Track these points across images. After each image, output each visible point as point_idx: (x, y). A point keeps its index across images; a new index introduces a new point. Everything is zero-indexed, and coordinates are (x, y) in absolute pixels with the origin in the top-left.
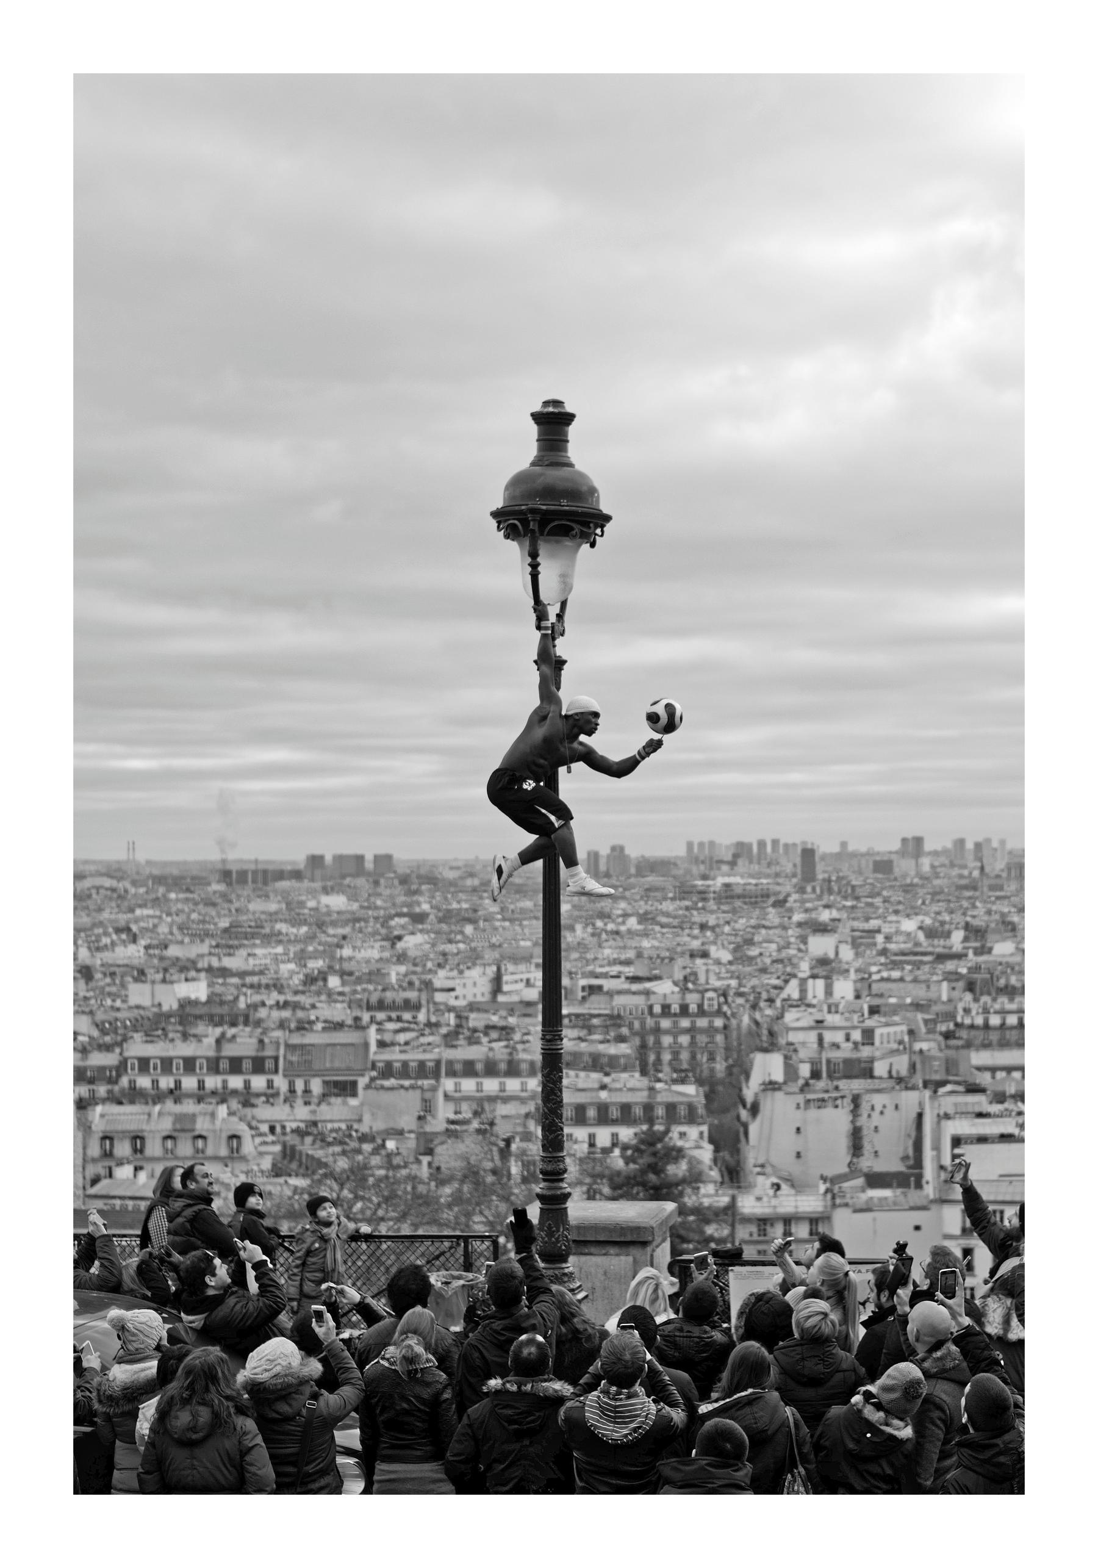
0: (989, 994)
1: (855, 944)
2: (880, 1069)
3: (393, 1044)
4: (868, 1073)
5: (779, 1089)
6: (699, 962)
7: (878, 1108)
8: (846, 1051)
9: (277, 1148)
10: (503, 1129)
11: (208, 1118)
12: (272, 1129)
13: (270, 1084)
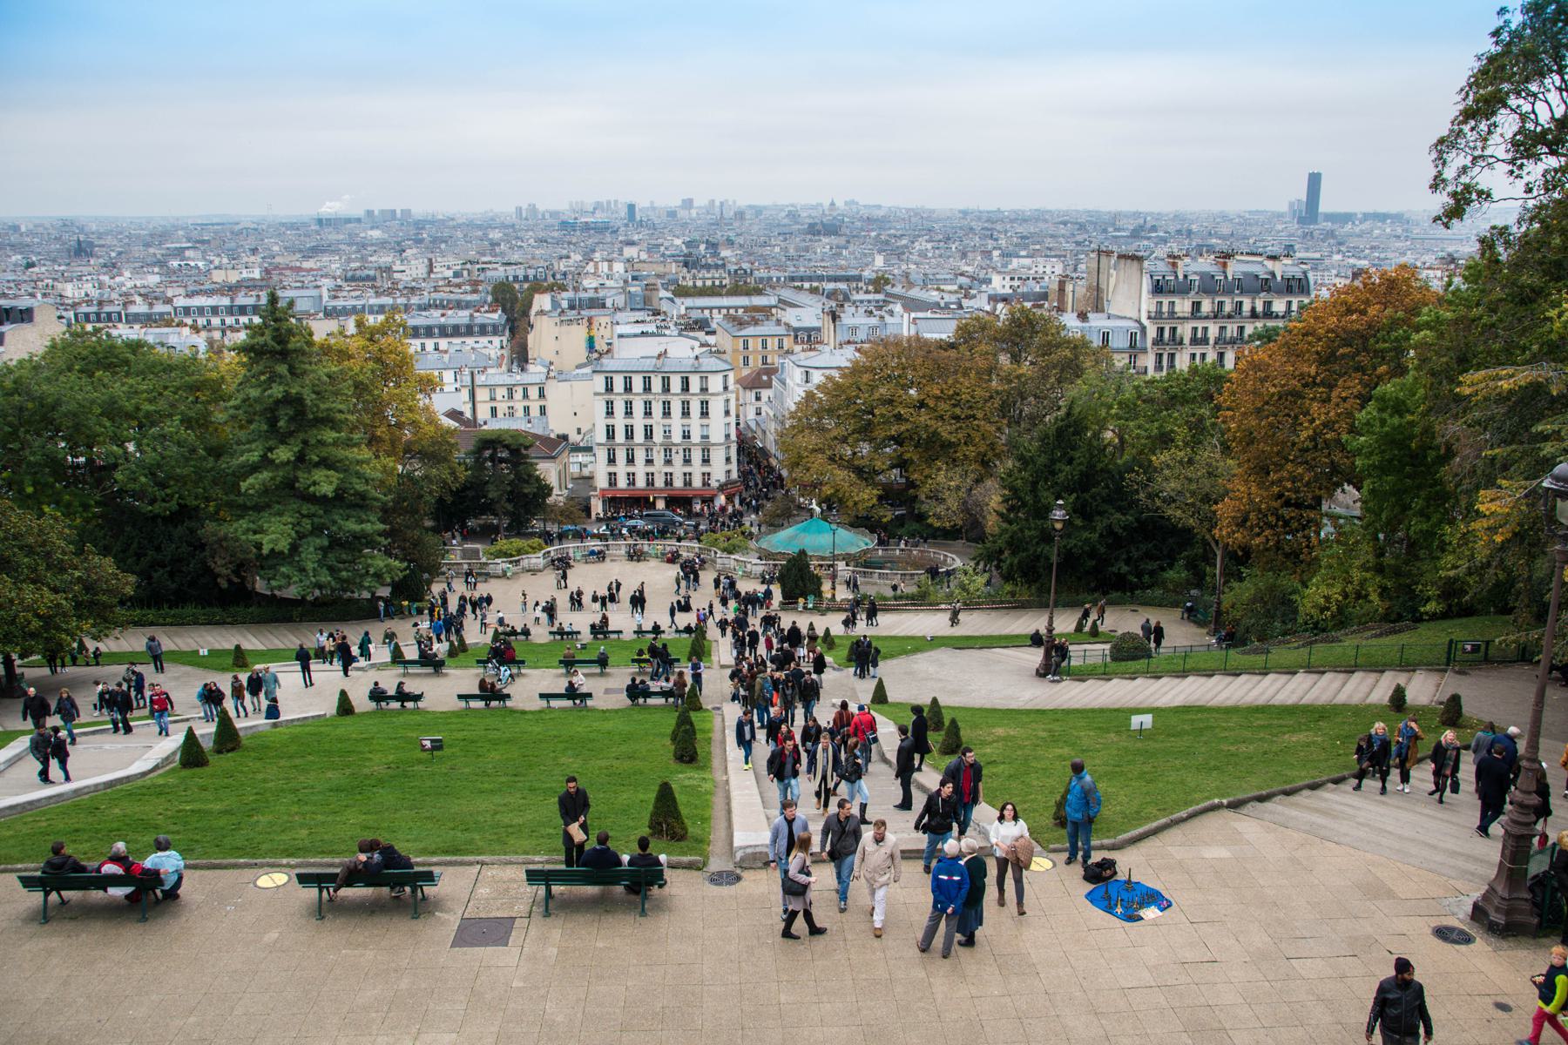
1: (649, 251)
2: (609, 303)
4: (604, 306)
7: (603, 325)
8: (591, 294)
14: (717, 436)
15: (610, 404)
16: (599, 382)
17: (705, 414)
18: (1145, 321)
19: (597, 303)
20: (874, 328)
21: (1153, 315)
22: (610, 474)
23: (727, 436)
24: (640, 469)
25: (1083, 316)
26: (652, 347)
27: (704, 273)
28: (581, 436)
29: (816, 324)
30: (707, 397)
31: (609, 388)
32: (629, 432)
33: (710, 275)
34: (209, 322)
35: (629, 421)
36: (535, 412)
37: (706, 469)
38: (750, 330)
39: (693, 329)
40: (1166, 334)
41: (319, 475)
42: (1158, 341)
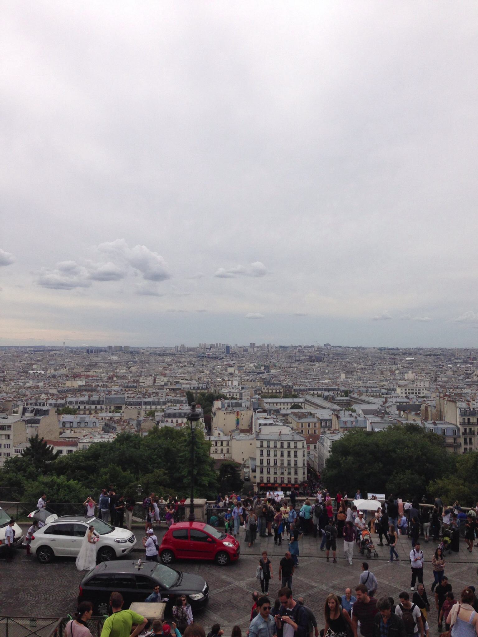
0: (269, 385)
2: (243, 405)
3: (130, 397)
5: (220, 410)
6: (202, 374)
7: (243, 414)
8: (236, 401)
9: (104, 424)
10: (157, 419)
11: (88, 418)
12: (102, 419)
13: (101, 407)
14: (300, 464)
15: (262, 452)
16: (258, 444)
17: (296, 456)
18: (459, 426)
19: (239, 405)
20: (353, 422)
21: (462, 423)
22: (261, 477)
23: (304, 464)
24: (272, 476)
25: (435, 423)
26: (275, 429)
27: (272, 387)
28: (244, 461)
29: (328, 418)
30: (297, 450)
31: (262, 446)
32: (268, 463)
33: (275, 388)
34: (79, 407)
35: (268, 458)
36: (225, 451)
37: (296, 477)
38: (303, 420)
39: (288, 423)
40: (468, 431)
41: (204, 478)
42: (465, 433)
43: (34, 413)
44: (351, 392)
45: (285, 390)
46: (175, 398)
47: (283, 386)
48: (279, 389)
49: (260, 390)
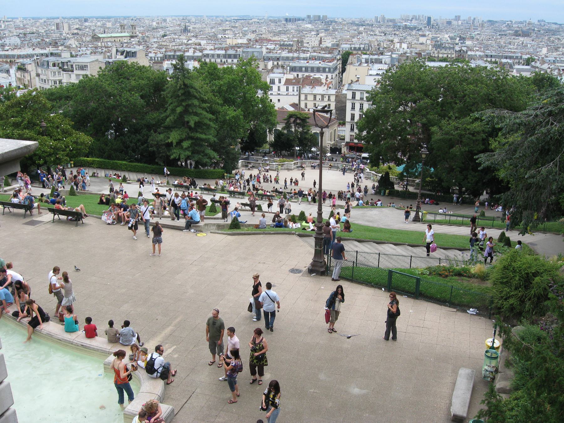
8: (376, 57)
22: (351, 136)
27: (443, 51)
31: (354, 97)
33: (446, 52)
43: (125, 54)
44: (533, 60)
45: (457, 55)
46: (320, 55)
47: (456, 50)
48: (452, 54)
49: (429, 54)
